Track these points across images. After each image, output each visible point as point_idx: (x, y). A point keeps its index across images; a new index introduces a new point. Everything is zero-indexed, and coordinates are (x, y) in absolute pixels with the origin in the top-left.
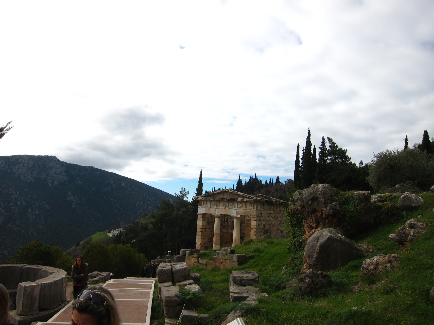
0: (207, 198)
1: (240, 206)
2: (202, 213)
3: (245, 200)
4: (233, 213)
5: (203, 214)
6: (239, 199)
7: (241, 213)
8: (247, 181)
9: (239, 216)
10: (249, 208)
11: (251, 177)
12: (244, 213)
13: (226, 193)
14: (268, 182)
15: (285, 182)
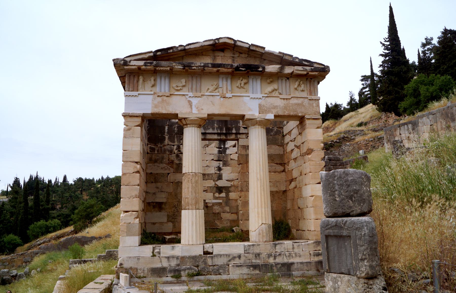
0: (163, 63)
1: (270, 88)
2: (141, 112)
3: (288, 70)
4: (250, 110)
5: (144, 117)
6: (272, 68)
7: (275, 107)
8: (27, 180)
9: (271, 116)
10: (298, 94)
11: (31, 176)
12: (285, 108)
13: (221, 54)
14: (53, 182)
15: (74, 181)
